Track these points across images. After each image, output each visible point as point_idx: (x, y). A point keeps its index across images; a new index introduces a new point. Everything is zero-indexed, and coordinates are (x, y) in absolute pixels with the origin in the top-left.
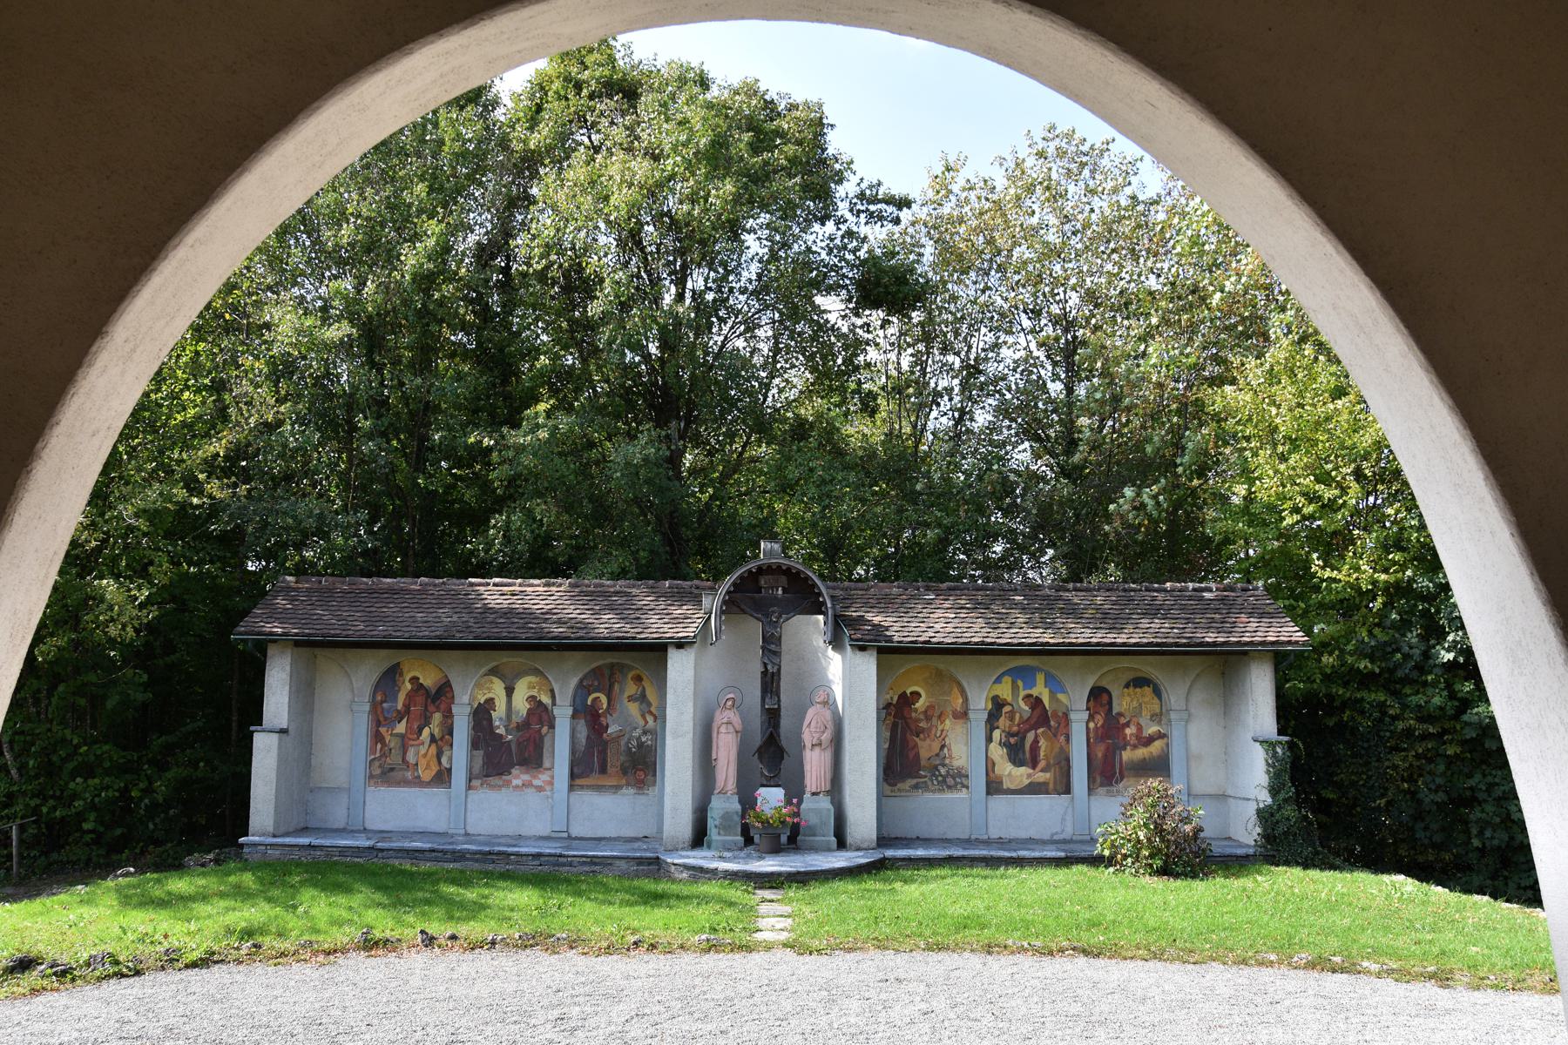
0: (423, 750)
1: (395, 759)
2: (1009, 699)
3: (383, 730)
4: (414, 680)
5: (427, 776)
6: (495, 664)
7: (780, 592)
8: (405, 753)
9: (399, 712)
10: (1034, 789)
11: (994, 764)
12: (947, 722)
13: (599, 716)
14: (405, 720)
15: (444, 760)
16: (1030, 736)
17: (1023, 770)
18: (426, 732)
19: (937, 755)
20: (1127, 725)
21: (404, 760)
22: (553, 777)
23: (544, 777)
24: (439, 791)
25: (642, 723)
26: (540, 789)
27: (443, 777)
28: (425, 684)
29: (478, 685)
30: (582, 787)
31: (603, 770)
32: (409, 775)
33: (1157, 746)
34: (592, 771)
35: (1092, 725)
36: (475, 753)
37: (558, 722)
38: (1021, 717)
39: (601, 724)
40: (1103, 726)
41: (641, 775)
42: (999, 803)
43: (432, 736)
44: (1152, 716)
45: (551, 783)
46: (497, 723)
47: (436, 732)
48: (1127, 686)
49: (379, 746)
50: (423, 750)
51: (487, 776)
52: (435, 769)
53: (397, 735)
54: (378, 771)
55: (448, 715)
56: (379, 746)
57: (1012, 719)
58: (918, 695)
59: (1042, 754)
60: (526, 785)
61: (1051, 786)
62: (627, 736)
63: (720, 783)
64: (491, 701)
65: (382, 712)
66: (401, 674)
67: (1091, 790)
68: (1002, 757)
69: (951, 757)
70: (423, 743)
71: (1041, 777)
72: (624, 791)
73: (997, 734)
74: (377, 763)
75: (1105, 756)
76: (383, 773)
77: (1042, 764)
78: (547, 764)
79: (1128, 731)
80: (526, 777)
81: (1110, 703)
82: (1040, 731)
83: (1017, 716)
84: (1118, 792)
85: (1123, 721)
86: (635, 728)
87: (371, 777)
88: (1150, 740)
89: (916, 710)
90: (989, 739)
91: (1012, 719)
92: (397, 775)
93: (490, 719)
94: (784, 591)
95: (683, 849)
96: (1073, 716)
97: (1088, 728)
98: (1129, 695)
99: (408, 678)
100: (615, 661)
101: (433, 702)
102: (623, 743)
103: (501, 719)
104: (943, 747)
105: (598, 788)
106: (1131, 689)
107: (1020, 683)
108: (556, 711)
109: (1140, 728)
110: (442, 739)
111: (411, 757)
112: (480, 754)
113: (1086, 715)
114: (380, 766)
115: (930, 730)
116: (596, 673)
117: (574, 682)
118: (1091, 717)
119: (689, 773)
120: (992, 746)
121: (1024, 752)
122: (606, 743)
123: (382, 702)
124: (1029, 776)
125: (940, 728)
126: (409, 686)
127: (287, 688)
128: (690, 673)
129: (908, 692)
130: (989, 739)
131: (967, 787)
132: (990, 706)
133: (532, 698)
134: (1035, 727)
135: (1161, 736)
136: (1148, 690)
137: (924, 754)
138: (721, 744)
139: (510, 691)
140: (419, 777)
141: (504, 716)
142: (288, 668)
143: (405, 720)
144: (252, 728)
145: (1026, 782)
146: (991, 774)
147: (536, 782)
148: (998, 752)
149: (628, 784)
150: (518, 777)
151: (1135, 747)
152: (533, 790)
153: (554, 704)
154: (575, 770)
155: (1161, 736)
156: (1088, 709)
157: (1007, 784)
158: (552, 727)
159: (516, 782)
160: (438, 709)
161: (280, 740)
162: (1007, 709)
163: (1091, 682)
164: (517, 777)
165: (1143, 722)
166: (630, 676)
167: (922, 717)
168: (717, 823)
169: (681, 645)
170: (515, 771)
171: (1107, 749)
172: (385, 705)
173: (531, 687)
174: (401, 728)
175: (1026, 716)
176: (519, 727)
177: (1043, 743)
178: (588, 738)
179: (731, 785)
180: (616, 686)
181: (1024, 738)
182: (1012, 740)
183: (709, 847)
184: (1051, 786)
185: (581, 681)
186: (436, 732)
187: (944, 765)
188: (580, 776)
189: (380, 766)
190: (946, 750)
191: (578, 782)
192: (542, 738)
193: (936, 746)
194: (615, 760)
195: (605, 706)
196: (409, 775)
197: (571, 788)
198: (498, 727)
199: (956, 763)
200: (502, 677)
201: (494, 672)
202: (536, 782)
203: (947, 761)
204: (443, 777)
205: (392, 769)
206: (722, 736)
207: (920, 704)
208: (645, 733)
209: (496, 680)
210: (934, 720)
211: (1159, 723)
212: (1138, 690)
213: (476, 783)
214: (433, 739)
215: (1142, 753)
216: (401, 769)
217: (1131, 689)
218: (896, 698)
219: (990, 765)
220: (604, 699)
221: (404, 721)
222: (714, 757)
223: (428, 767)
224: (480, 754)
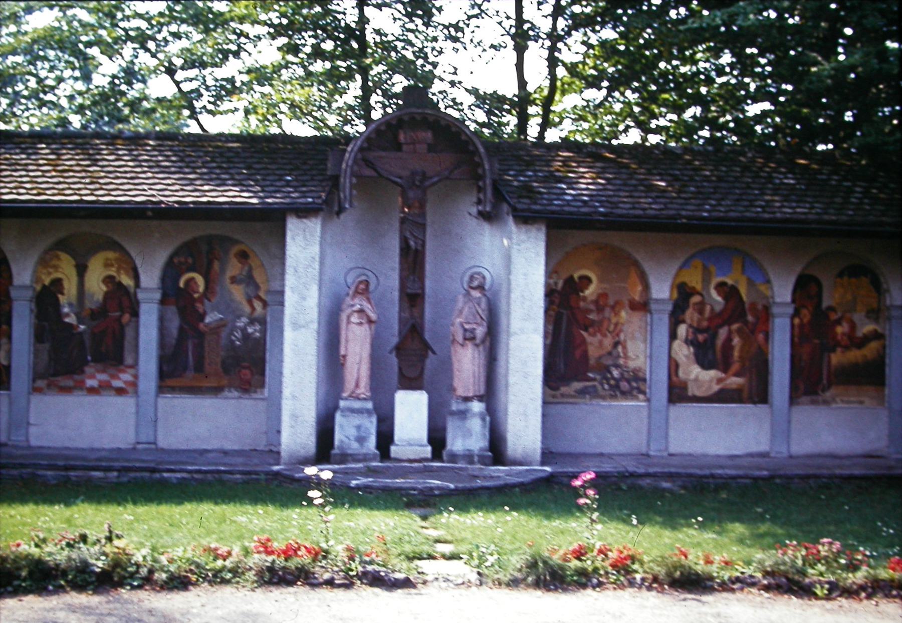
2: (699, 287)
6: (62, 234)
10: (723, 396)
11: (677, 366)
12: (623, 314)
16: (723, 333)
17: (713, 373)
19: (610, 353)
20: (838, 322)
22: (136, 377)
23: (127, 377)
25: (247, 309)
26: (120, 391)
33: (874, 345)
38: (712, 309)
42: (681, 411)
45: (134, 384)
46: (66, 310)
48: (840, 275)
57: (701, 312)
58: (587, 280)
59: (736, 354)
61: (745, 394)
63: (350, 385)
67: (794, 399)
68: (687, 357)
69: (626, 357)
71: (734, 381)
72: (226, 393)
73: (682, 330)
77: (735, 367)
78: (129, 360)
79: (839, 330)
80: (103, 377)
81: (819, 296)
82: (735, 326)
83: (708, 308)
85: (834, 317)
89: (584, 299)
90: (673, 336)
91: (701, 312)
93: (57, 305)
96: (775, 310)
97: (793, 326)
103: (70, 305)
104: (616, 344)
106: (845, 278)
107: (713, 269)
108: (141, 296)
109: (853, 326)
113: (790, 310)
115: (601, 322)
120: (677, 344)
121: (714, 353)
124: (719, 381)
125: (614, 320)
129: (576, 276)
130: (673, 336)
131: (644, 393)
132: (675, 295)
133: (109, 280)
134: (728, 322)
136: (865, 281)
137: (593, 352)
138: (351, 336)
139: (82, 270)
145: (716, 388)
146: (674, 379)
147: (117, 383)
148: (683, 352)
149: (230, 386)
151: (846, 348)
154: (165, 368)
155: (877, 336)
157: (692, 390)
158: (135, 314)
162: (696, 299)
164: (93, 377)
167: (592, 307)
170: (89, 370)
173: (107, 265)
175: (718, 308)
176: (95, 315)
177: (736, 341)
180: (216, 265)
181: (715, 335)
182: (701, 337)
184: (745, 394)
187: (617, 366)
190: (620, 349)
191: (170, 382)
192: (122, 328)
193: (608, 342)
195: (201, 289)
198: (67, 315)
199: (632, 364)
201: (62, 245)
203: (621, 361)
206: (354, 327)
207: (590, 292)
208: (252, 321)
209: (64, 256)
210: (607, 312)
211: (876, 320)
212: (853, 280)
215: (854, 355)
217: (845, 278)
218: (560, 284)
219: (673, 366)
220: (200, 280)
222: (342, 352)
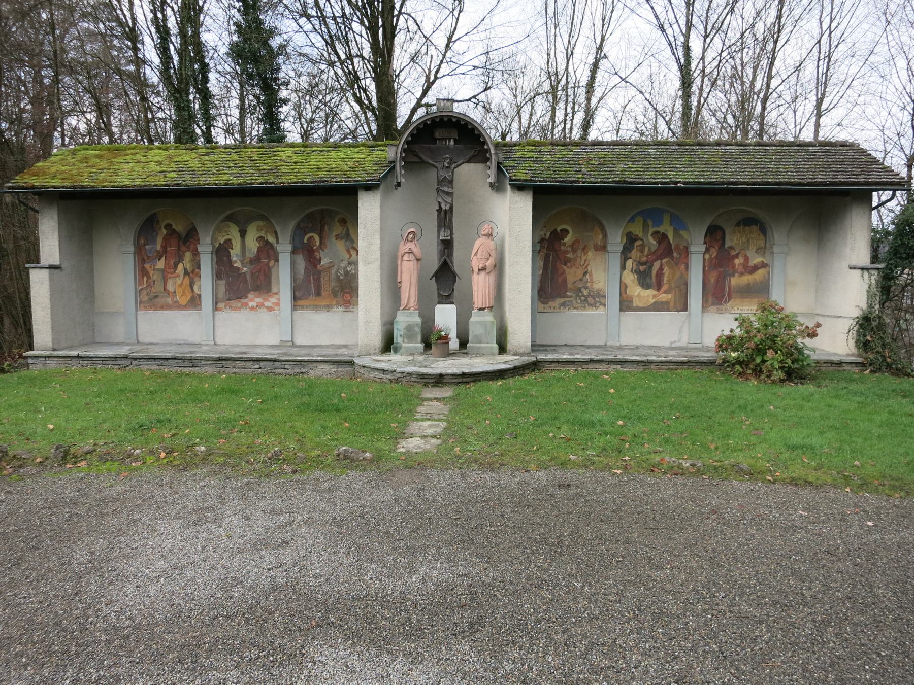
0: (179, 281)
1: (158, 288)
2: (640, 235)
3: (147, 266)
4: (168, 226)
5: (184, 301)
6: (229, 212)
7: (452, 143)
8: (165, 284)
9: (158, 252)
10: (658, 307)
11: (626, 287)
12: (590, 253)
13: (313, 251)
14: (164, 257)
15: (195, 288)
16: (657, 265)
17: (650, 292)
18: (180, 267)
19: (581, 280)
20: (737, 256)
21: (165, 289)
22: (279, 299)
23: (273, 300)
24: (192, 313)
25: (347, 256)
26: (270, 309)
27: (195, 302)
28: (177, 230)
29: (218, 229)
30: (302, 307)
31: (318, 294)
32: (169, 300)
33: (761, 272)
34: (310, 295)
35: (707, 256)
36: (220, 282)
37: (281, 256)
38: (649, 249)
39: (315, 258)
40: (716, 257)
41: (348, 297)
42: (630, 317)
43: (185, 269)
44: (757, 249)
45: (278, 304)
46: (234, 259)
47: (188, 267)
48: (738, 225)
49: (145, 279)
50: (179, 281)
51: (229, 300)
52: (189, 296)
53: (159, 270)
54: (146, 298)
55: (196, 254)
56: (145, 279)
57: (642, 251)
58: (565, 232)
59: (665, 279)
60: (260, 306)
61: (672, 305)
62: (336, 267)
63: (404, 302)
64: (229, 241)
65: (146, 252)
66: (158, 222)
67: (704, 308)
68: (633, 281)
69: (592, 282)
70: (178, 276)
71: (664, 297)
72: (335, 309)
73: (629, 263)
74: (145, 292)
75: (717, 281)
76: (150, 300)
77: (665, 287)
78: (274, 290)
79: (737, 261)
80: (259, 300)
81: (723, 239)
82: (665, 261)
83: (647, 249)
84: (726, 310)
85: (733, 253)
86: (342, 261)
87: (141, 302)
88: (755, 268)
89: (564, 244)
90: (623, 267)
91: (642, 251)
92: (161, 301)
93: (229, 256)
94: (456, 142)
95: (375, 354)
96: (692, 249)
97: (704, 259)
98: (739, 232)
99: (163, 226)
100: (324, 207)
101: (184, 243)
102: (333, 272)
103: (237, 255)
104: (585, 273)
105: (315, 308)
106: (742, 227)
107: (650, 223)
108: (279, 248)
109: (747, 259)
110: (193, 272)
111: (170, 287)
112: (222, 283)
113: (703, 248)
114: (147, 294)
115: (575, 259)
116: (310, 217)
117: (292, 225)
118: (707, 250)
119: (378, 293)
120: (625, 272)
121: (651, 277)
122: (320, 272)
123: (145, 245)
124: (654, 296)
125: (584, 258)
126: (164, 231)
127: (57, 233)
128: (377, 211)
129: (558, 229)
130: (623, 267)
131: (604, 305)
132: (625, 241)
133: (260, 239)
134: (660, 258)
135: (764, 265)
136: (755, 229)
137: (570, 279)
138: (404, 269)
139: (243, 233)
140: (177, 302)
141: (239, 253)
142: (56, 217)
143: (164, 257)
144: (27, 265)
145: (652, 301)
146: (624, 295)
147: (267, 304)
148: (630, 278)
149: (338, 304)
150: (253, 300)
151: (742, 274)
152: (265, 310)
153: (278, 242)
154: (297, 294)
155: (764, 265)
156: (705, 243)
157: (636, 303)
158: (277, 260)
159: (251, 304)
160: (188, 249)
161: (50, 274)
162: (638, 243)
163: (708, 222)
164: (252, 300)
165: (749, 254)
166: (336, 220)
167: (569, 249)
168: (401, 333)
169: (369, 187)
170: (250, 296)
171: (719, 276)
172: (147, 247)
173: (259, 229)
174: (161, 264)
175: (653, 249)
176: (251, 261)
177: (666, 271)
178: (306, 268)
179: (413, 303)
180: (326, 228)
181: (651, 267)
182: (642, 268)
183: (396, 351)
184: (672, 305)
185: (298, 224)
186: (188, 267)
187: (586, 288)
188: (300, 299)
189: (147, 294)
190: (588, 276)
191: (300, 303)
192: (270, 269)
193: (580, 272)
194: (327, 285)
195: (318, 244)
196: (169, 300)
197: (294, 307)
198: (236, 262)
199: (596, 286)
200: (237, 223)
201: (230, 218)
202: (267, 304)
203: (589, 285)
204: (195, 302)
205: (157, 297)
206: (405, 263)
207: (568, 239)
208: (350, 264)
209: (231, 224)
210: (579, 252)
211: (763, 255)
212: (747, 228)
213: (221, 305)
214: (186, 272)
215: (747, 279)
216: (163, 297)
217: (742, 227)
218: (548, 234)
219: (623, 287)
220: (317, 238)
221: (163, 259)
222: (399, 280)
223: (184, 294)
224: (222, 283)
